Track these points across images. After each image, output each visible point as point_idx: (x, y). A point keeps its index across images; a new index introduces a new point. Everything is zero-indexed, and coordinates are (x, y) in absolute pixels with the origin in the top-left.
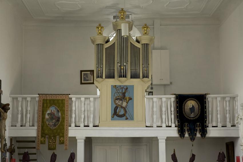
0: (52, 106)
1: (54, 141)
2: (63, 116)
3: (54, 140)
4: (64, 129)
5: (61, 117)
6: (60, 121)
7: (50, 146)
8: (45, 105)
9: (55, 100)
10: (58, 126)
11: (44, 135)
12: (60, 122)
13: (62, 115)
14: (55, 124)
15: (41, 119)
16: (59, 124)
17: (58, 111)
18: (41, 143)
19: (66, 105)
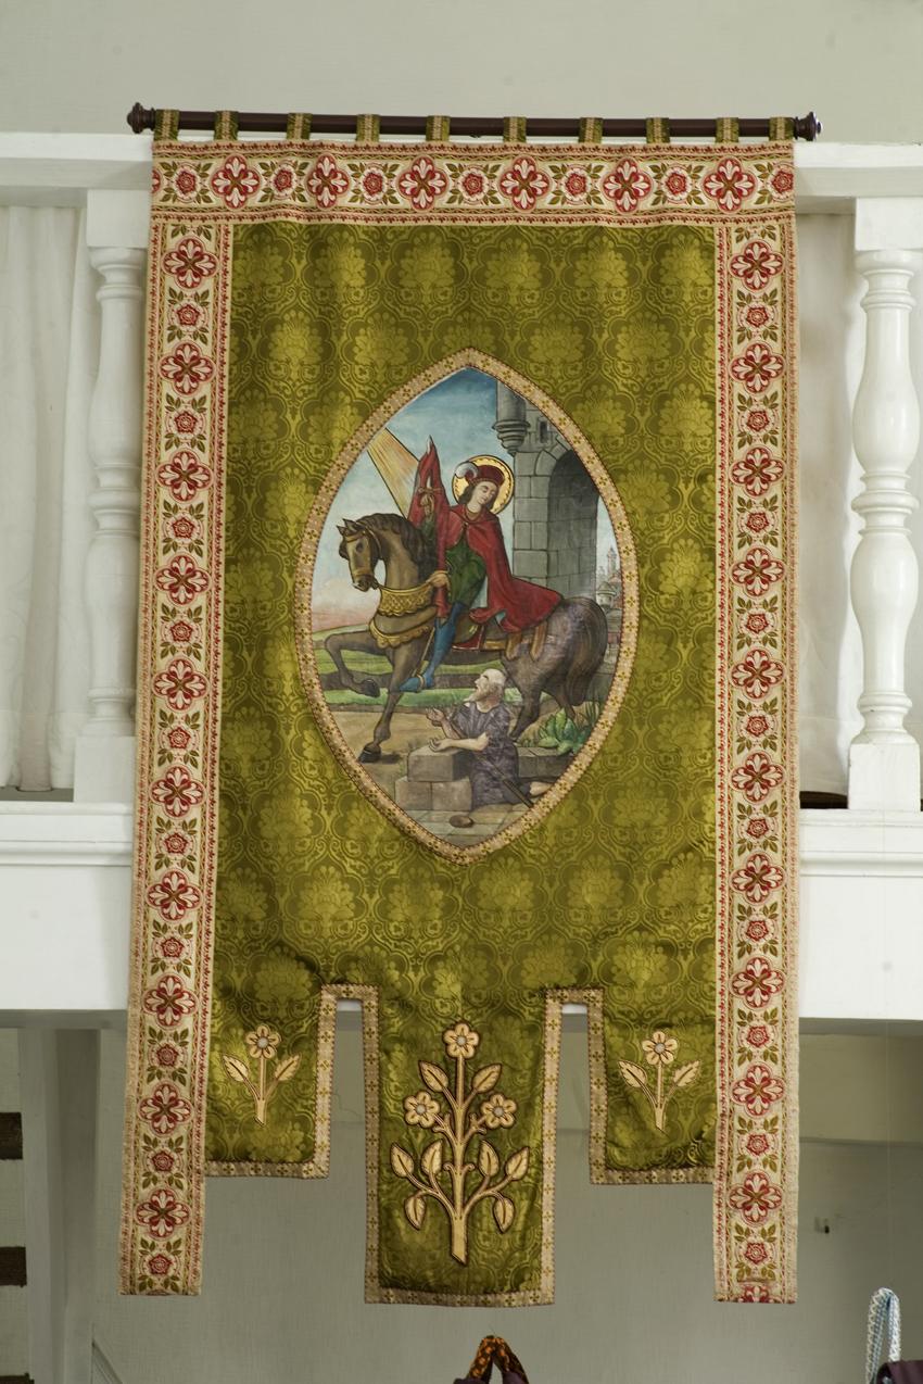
0: (440, 372)
1: (499, 1112)
2: (681, 570)
3: (486, 1079)
4: (696, 854)
5: (632, 613)
6: (619, 690)
7: (415, 1208)
8: (294, 346)
9: (508, 239)
10: (577, 791)
11: (287, 978)
12: (610, 713)
13: (650, 556)
14: (504, 746)
15: (208, 635)
16: (583, 760)
17: (570, 462)
18: (217, 1155)
19: (726, 349)
